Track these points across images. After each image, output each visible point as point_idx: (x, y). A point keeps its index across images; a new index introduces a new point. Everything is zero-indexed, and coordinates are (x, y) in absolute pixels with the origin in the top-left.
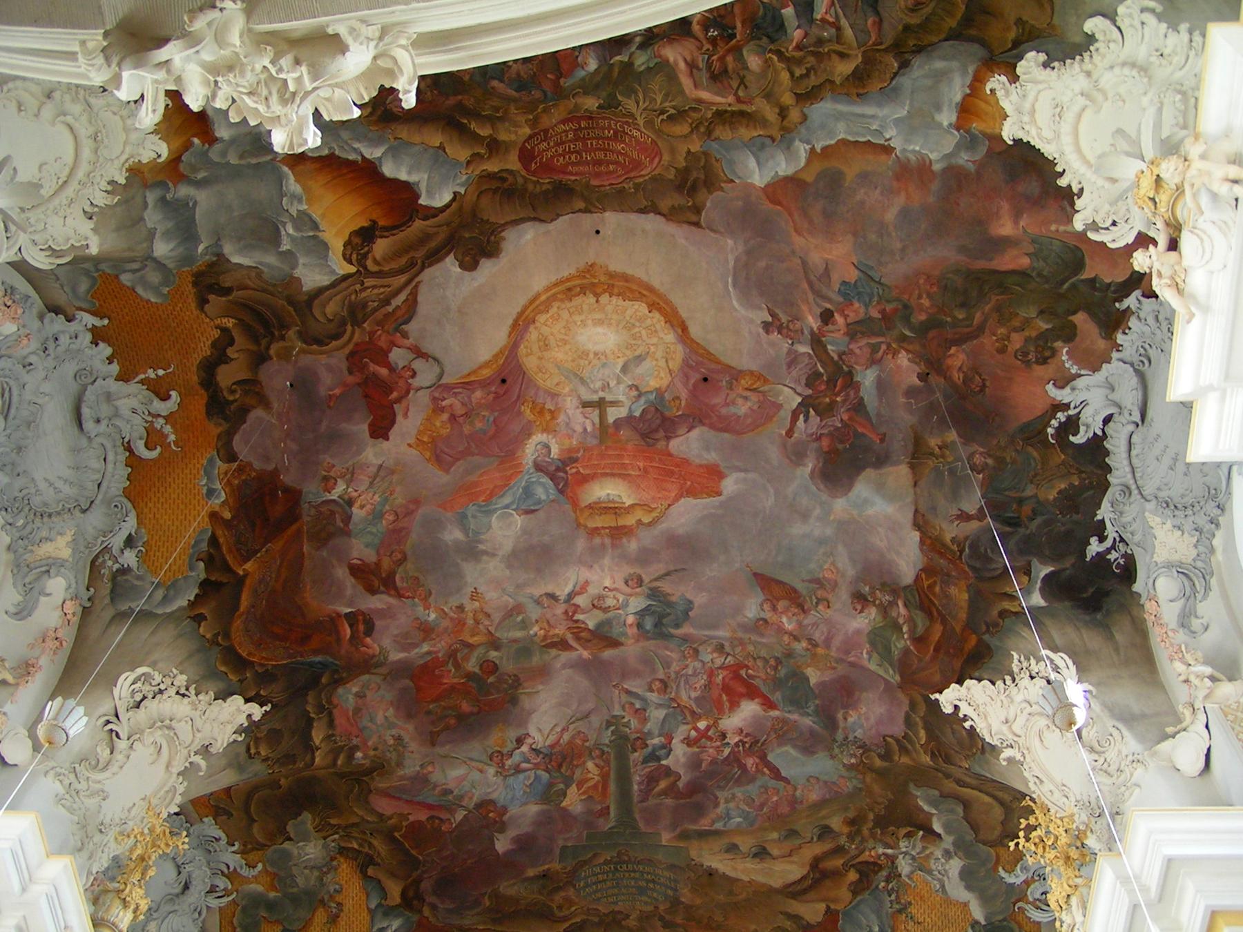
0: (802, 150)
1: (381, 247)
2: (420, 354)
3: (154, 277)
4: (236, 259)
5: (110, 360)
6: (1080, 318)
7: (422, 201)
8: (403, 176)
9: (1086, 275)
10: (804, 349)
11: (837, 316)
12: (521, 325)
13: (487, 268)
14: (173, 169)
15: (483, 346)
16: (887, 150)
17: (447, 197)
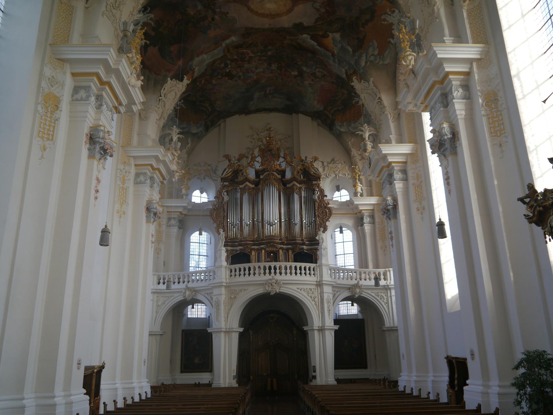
0: (224, 45)
1: (321, 33)
2: (318, 10)
3: (371, 50)
4: (351, 50)
5: (393, 29)
6: (153, 34)
7: (309, 37)
8: (313, 42)
9: (157, 47)
10: (218, 10)
11: (210, 20)
12: (290, 11)
13: (297, 21)
14: (355, 73)
15: (300, 8)
16: (206, 54)
17: (304, 35)
